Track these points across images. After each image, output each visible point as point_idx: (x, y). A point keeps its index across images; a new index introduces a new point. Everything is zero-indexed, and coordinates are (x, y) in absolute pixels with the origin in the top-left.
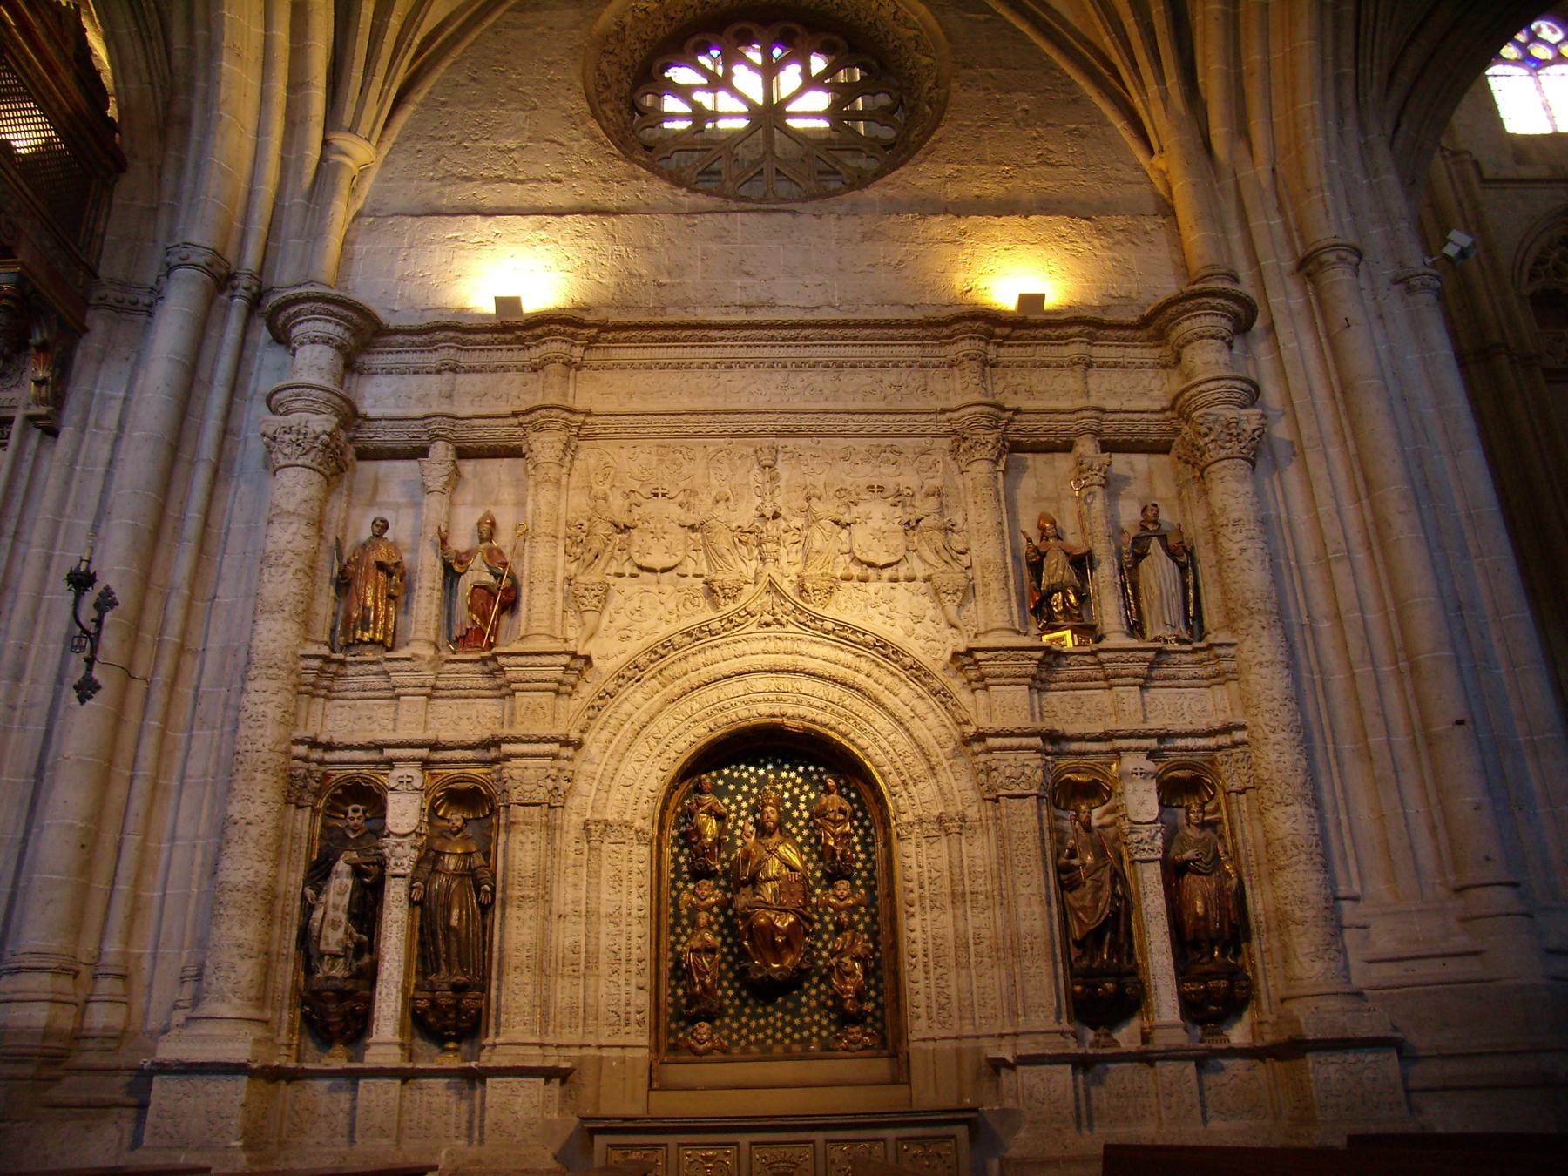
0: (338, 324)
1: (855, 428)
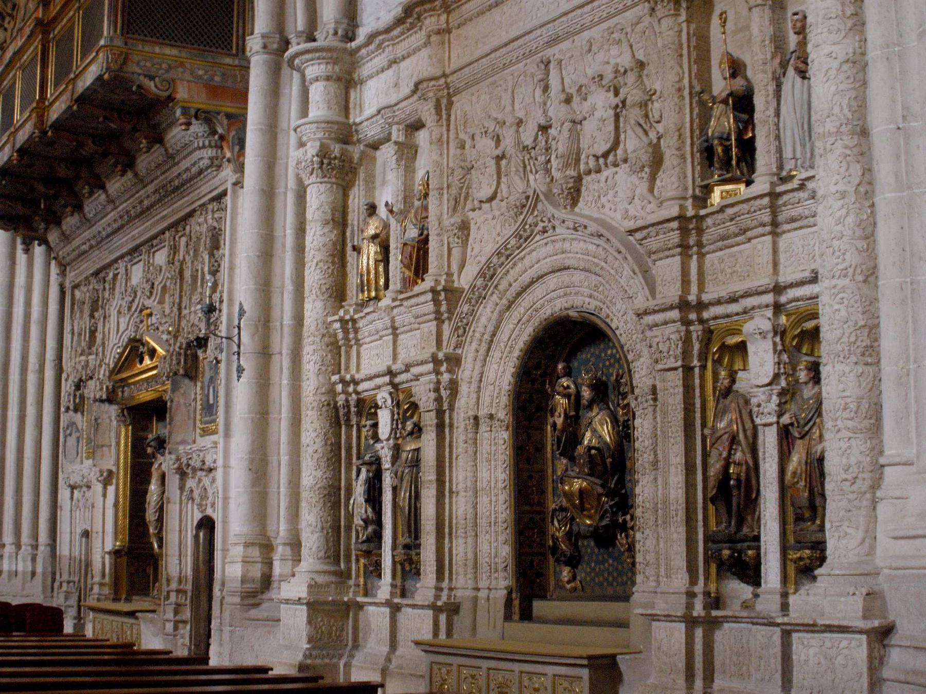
0: (319, 64)
1: (590, 18)
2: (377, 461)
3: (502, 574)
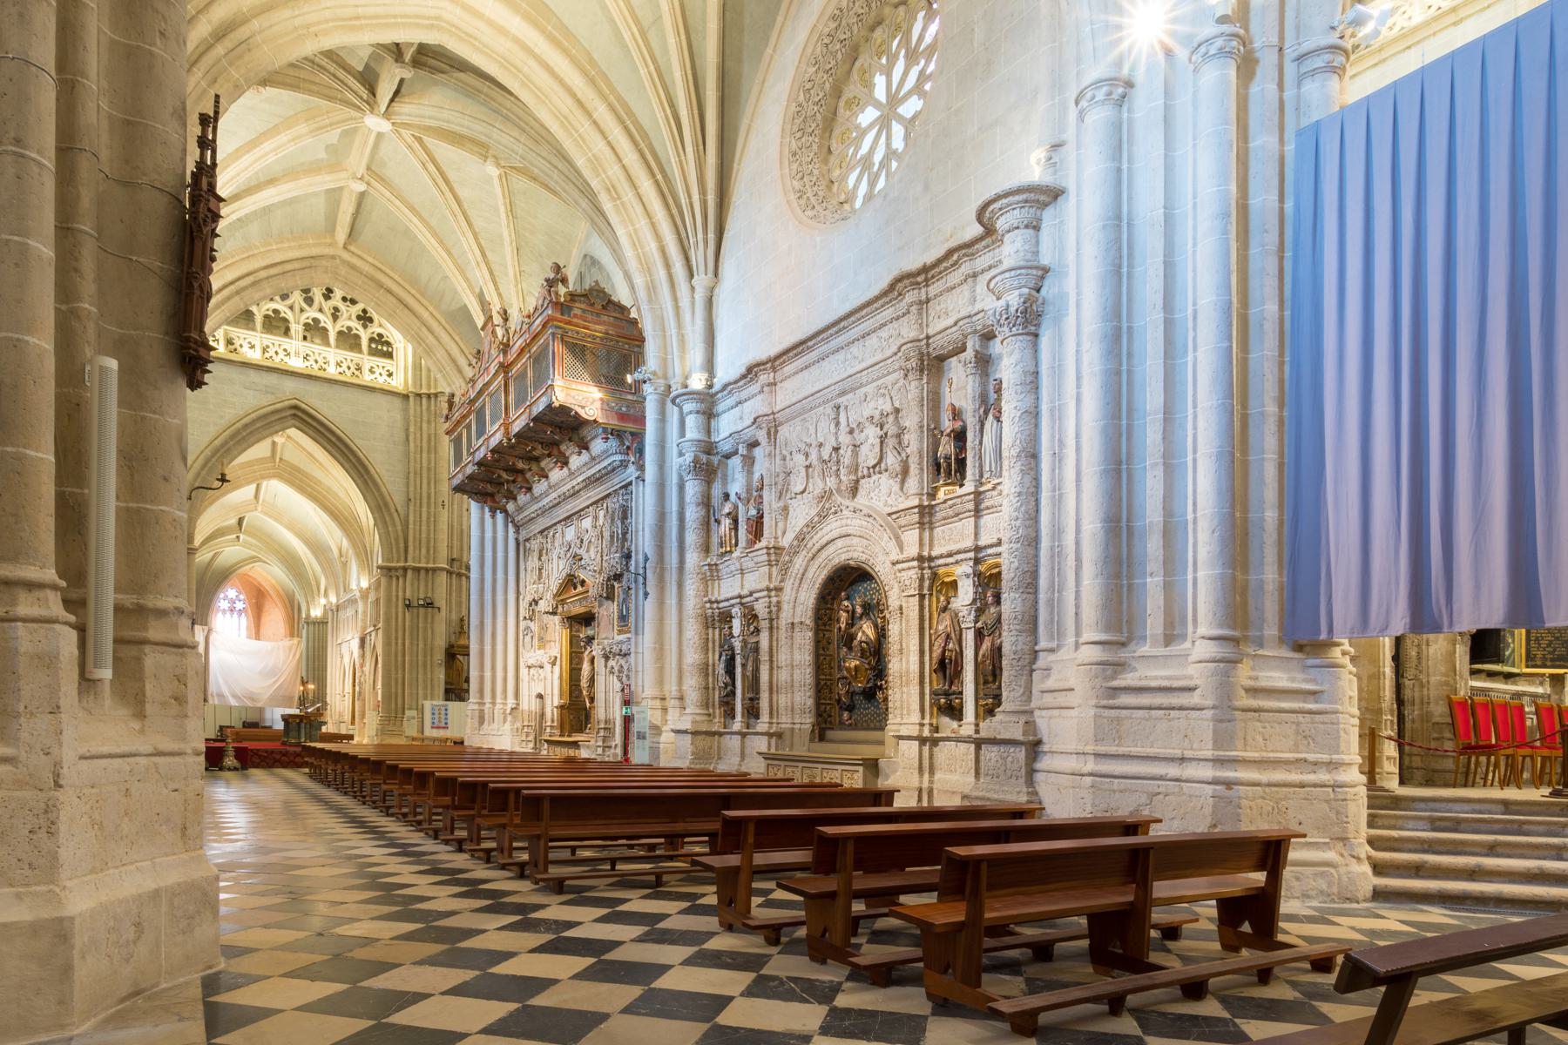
2: (732, 649)
3: (807, 715)
